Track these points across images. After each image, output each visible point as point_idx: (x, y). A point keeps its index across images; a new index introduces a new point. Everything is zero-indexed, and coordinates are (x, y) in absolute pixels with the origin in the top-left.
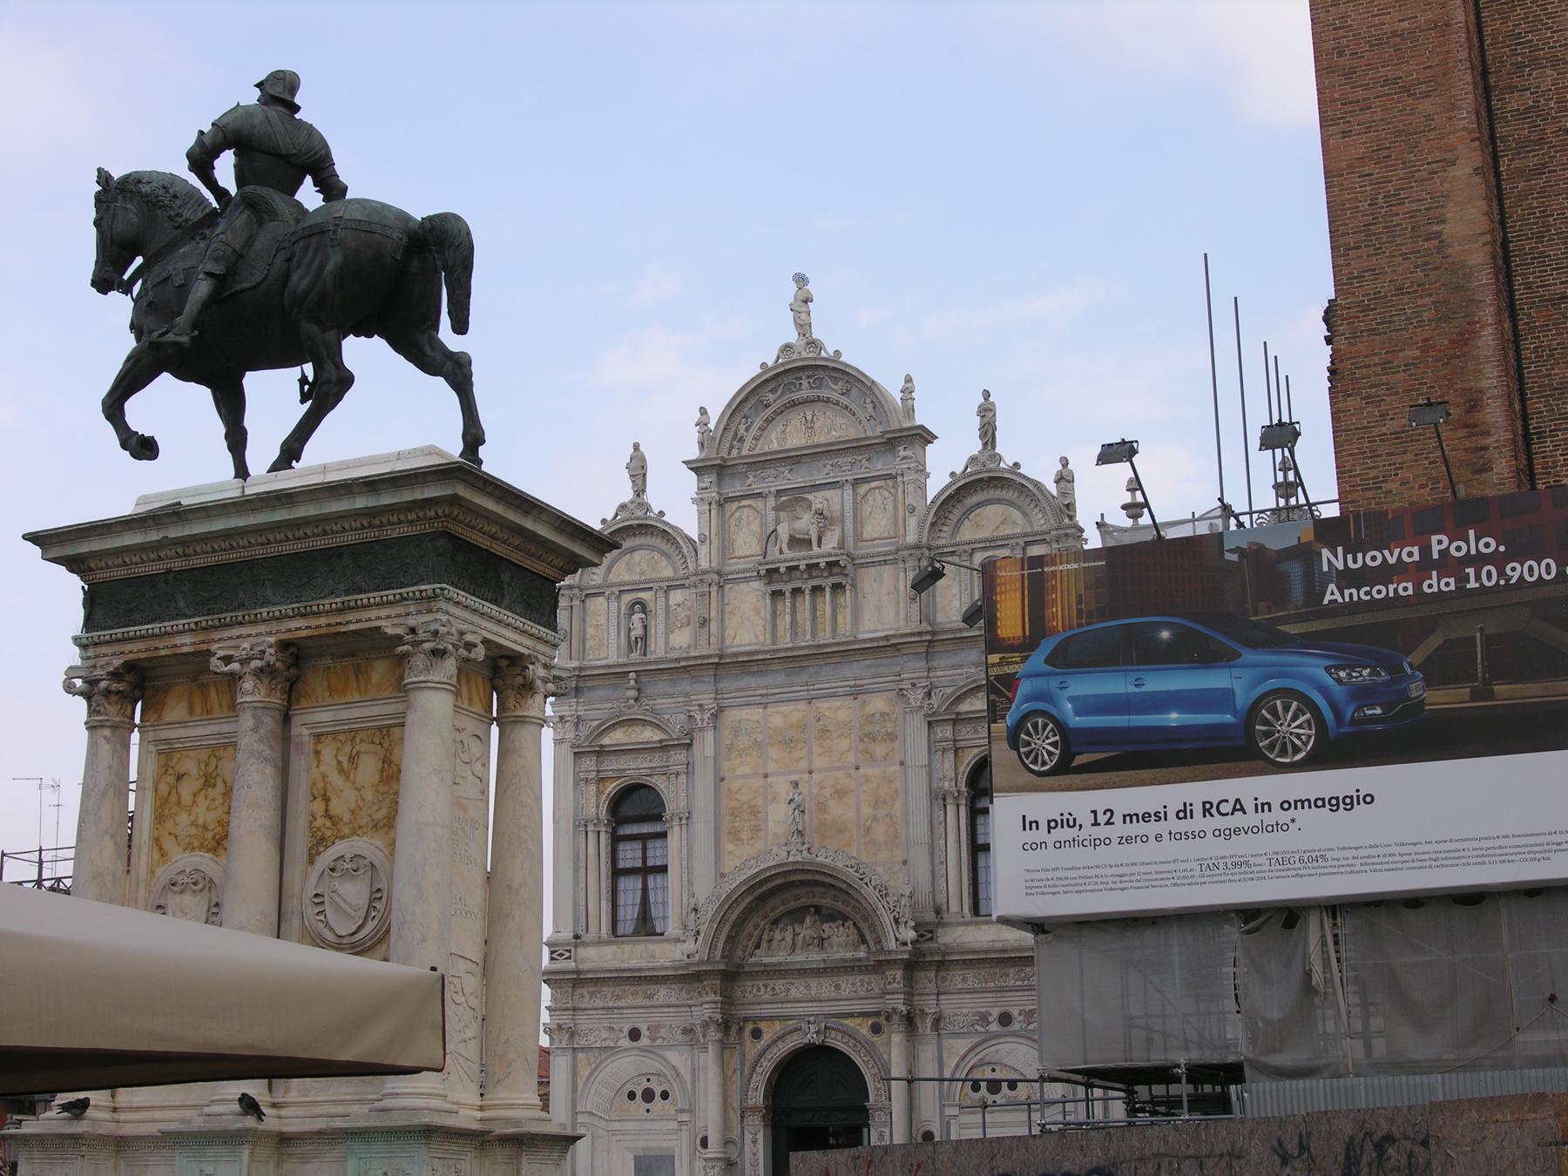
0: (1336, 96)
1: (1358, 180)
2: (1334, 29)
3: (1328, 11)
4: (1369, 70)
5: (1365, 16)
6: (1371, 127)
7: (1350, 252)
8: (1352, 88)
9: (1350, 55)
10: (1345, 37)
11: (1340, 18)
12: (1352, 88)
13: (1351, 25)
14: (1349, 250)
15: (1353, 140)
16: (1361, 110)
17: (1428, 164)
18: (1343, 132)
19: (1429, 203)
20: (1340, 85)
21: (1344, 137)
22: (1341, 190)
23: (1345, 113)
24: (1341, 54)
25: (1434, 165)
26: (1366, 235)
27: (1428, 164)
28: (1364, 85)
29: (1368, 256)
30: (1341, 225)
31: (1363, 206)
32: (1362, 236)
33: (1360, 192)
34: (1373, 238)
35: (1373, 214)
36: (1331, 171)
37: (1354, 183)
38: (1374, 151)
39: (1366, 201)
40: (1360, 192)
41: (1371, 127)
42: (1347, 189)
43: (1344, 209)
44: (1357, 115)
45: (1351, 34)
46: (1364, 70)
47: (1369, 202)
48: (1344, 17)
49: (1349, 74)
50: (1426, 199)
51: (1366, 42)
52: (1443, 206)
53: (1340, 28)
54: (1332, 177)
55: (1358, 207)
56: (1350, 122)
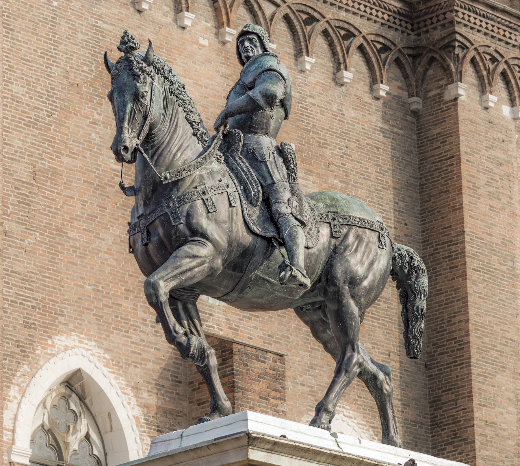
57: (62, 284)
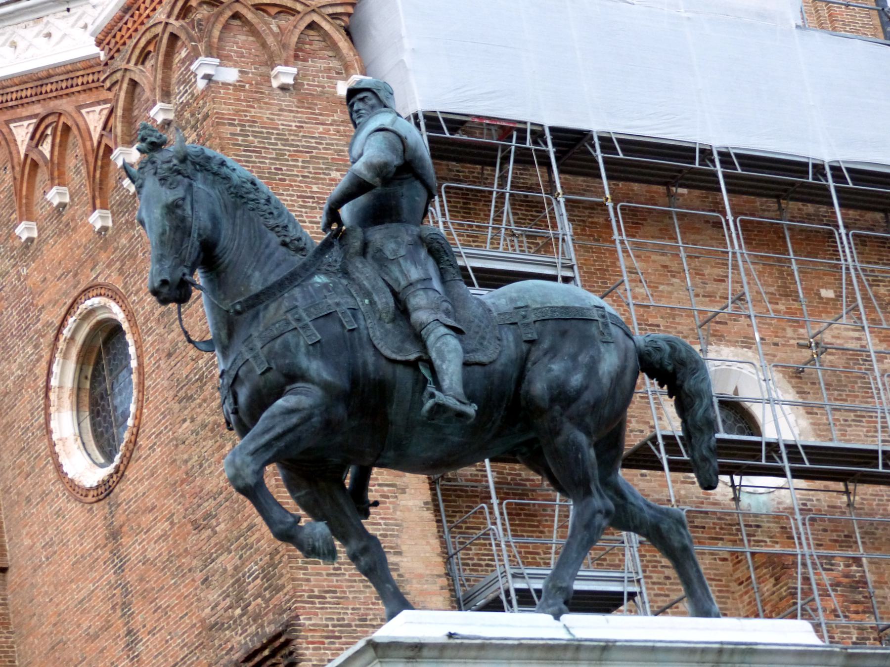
7: (309, 566)
17: (380, 485)
19: (384, 530)
25: (386, 489)
27: (380, 485)
29: (328, 575)
50: (379, 524)
52: (397, 536)
57: (541, 528)
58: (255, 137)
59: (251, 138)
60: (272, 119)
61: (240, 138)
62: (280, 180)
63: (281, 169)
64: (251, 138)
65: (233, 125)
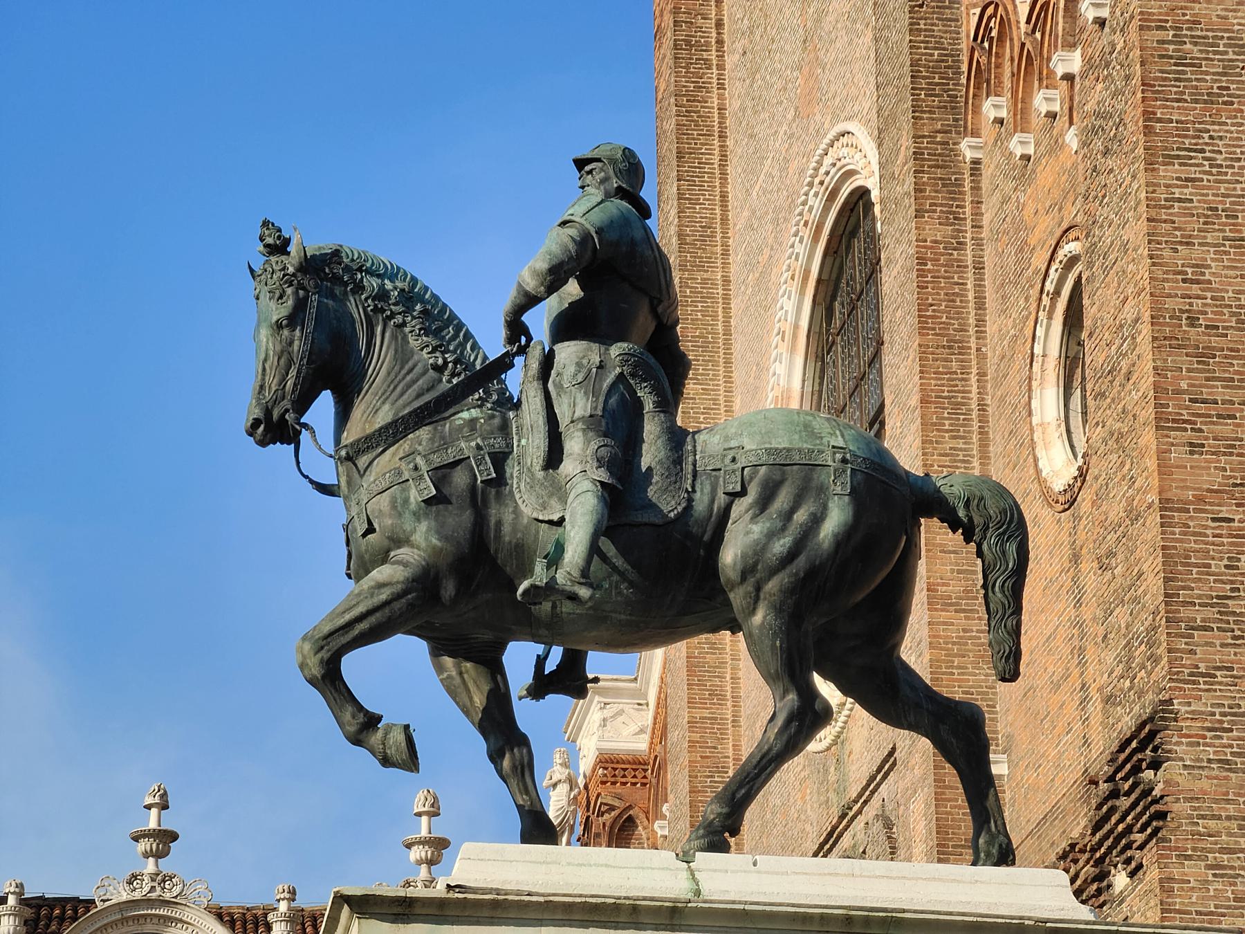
0: (1184, 385)
1: (1210, 523)
2: (1184, 281)
3: (1176, 251)
4: (1234, 358)
5: (1231, 273)
6: (1233, 446)
8: (1208, 379)
9: (1207, 327)
10: (1198, 297)
11: (1194, 266)
12: (1208, 379)
13: (1210, 282)
14: (1193, 628)
15: (1207, 461)
16: (1219, 416)
18: (1191, 445)
20: (1189, 370)
21: (1192, 453)
22: (1185, 534)
23: (1193, 415)
24: (1193, 322)
26: (1219, 612)
28: (1224, 380)
29: (1222, 645)
30: (1184, 588)
31: (1217, 566)
32: (1211, 613)
33: (1213, 544)
34: (1231, 619)
35: (1232, 582)
36: (1168, 500)
37: (1206, 527)
38: (1236, 485)
39: (1221, 559)
40: (1213, 544)
41: (1233, 446)
42: (1194, 534)
43: (1189, 565)
44: (1213, 423)
45: (1209, 295)
46: (1226, 357)
47: (1226, 562)
48: (1201, 266)
49: (1205, 355)
51: (1233, 314)
53: (1192, 282)
54: (1171, 510)
55: (1209, 566)
56: (1201, 430)
58: (1196, 44)
59: (1188, 46)
60: (1226, 18)
61: (1172, 47)
62: (1225, 103)
63: (1228, 88)
64: (1188, 46)
65: (1165, 29)
